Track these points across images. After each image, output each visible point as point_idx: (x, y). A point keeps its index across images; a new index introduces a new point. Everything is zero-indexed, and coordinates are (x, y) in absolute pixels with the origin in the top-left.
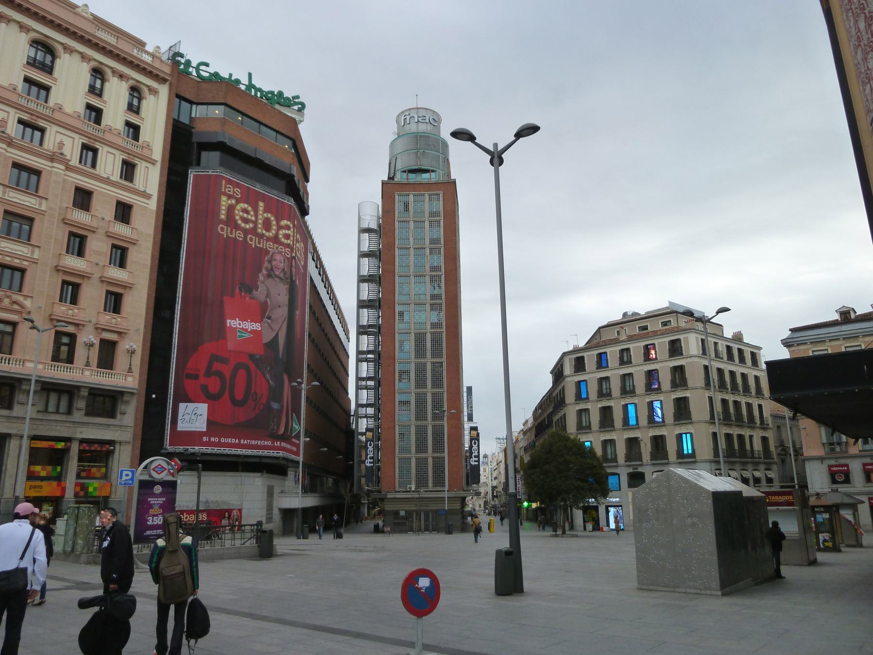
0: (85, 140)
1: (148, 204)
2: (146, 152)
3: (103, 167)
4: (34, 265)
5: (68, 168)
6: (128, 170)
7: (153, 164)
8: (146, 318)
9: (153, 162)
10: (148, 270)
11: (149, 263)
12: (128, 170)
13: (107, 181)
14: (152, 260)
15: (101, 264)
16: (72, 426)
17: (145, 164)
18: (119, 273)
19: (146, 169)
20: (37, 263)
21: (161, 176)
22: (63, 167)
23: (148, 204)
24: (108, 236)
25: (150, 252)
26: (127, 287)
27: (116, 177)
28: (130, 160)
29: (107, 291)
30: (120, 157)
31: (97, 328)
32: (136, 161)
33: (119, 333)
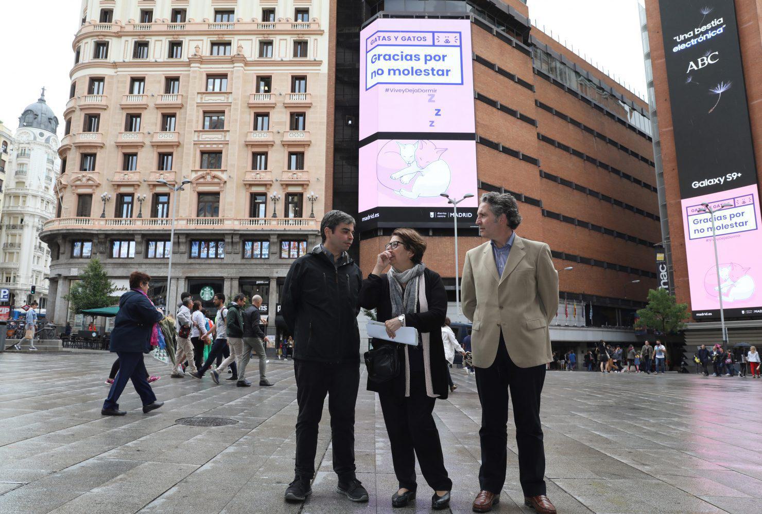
0: (261, 38)
1: (320, 70)
2: (314, 27)
3: (277, 53)
4: (227, 145)
5: (247, 64)
6: (301, 47)
7: (321, 34)
8: (327, 168)
9: (321, 33)
10: (324, 127)
11: (325, 120)
12: (301, 47)
13: (282, 63)
14: (327, 116)
15: (281, 131)
16: (269, 267)
17: (313, 37)
18: (297, 135)
19: (316, 41)
20: (228, 144)
21: (330, 41)
22: (242, 65)
23: (320, 70)
24: (286, 107)
25: (325, 110)
26: (307, 144)
27: (289, 56)
28: (301, 39)
29: (289, 152)
30: (290, 40)
31: (282, 185)
32: (305, 38)
33: (302, 185)
